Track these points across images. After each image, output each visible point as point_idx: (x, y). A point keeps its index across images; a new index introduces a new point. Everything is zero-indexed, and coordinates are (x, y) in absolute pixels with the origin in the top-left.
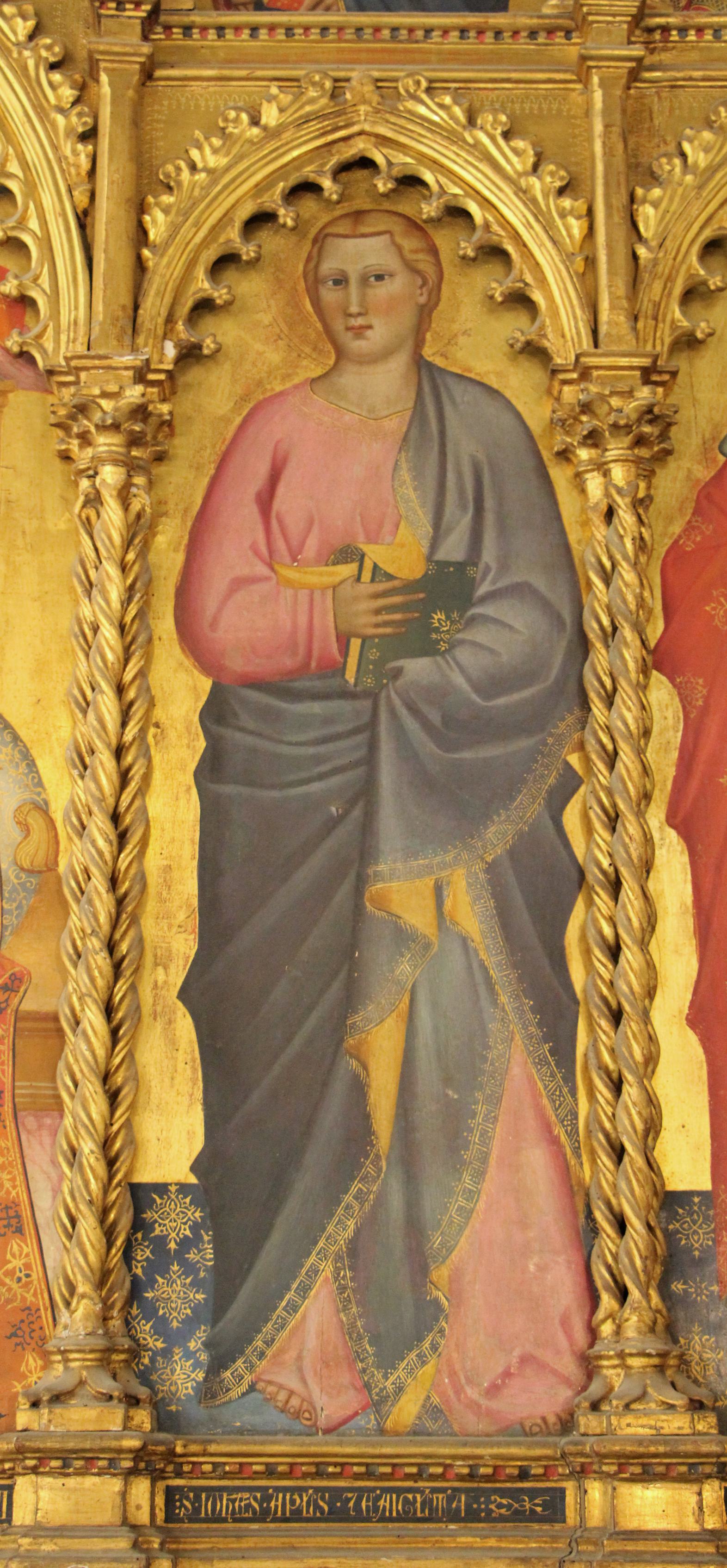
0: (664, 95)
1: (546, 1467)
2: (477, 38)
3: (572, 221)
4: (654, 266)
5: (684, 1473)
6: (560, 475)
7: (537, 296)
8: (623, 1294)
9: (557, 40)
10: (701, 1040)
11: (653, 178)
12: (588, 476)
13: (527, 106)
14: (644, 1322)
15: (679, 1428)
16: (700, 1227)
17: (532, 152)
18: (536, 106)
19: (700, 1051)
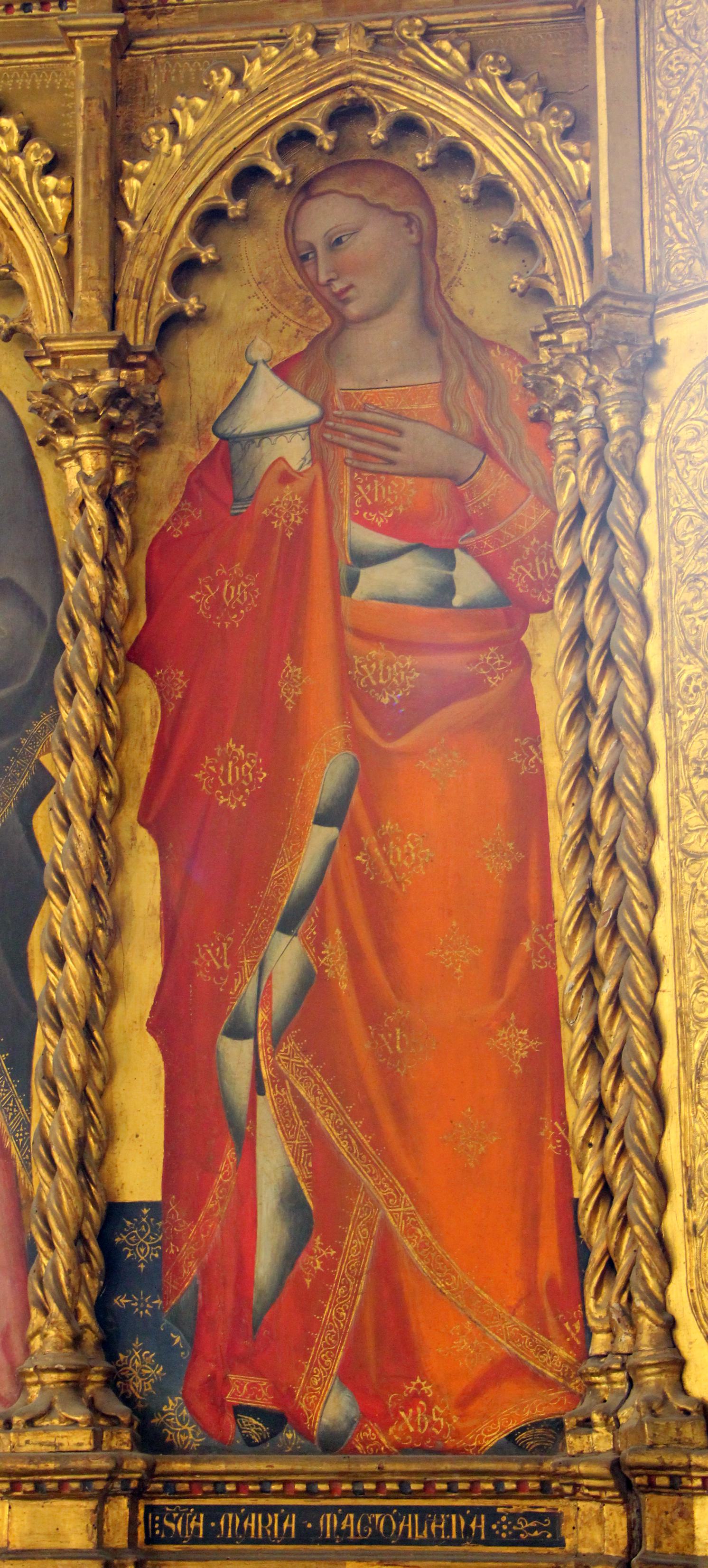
0: (160, 61)
3: (54, 199)
4: (136, 243)
5: (77, 1490)
7: (22, 279)
9: (52, 11)
10: (160, 1046)
11: (141, 151)
12: (66, 465)
13: (19, 82)
14: (61, 1337)
15: (80, 1444)
16: (148, 1239)
17: (16, 131)
18: (29, 82)
19: (160, 1057)
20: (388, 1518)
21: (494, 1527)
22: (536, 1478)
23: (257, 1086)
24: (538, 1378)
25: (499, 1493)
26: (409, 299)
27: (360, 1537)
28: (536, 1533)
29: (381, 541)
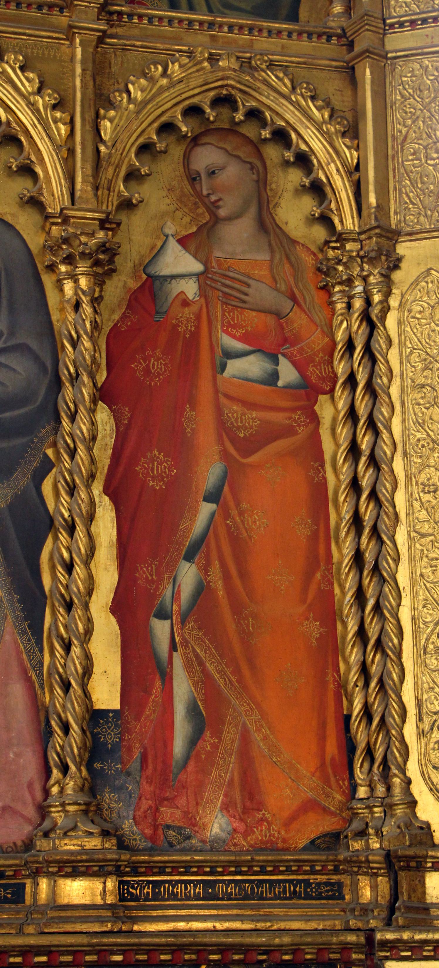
0: (118, 53)
1: (15, 871)
2: (5, 5)
4: (109, 158)
5: (96, 871)
6: (48, 280)
7: (38, 170)
8: (65, 769)
9: (55, 13)
10: (117, 621)
11: (110, 104)
12: (65, 282)
13: (35, 51)
14: (77, 785)
15: (95, 846)
16: (112, 731)
17: (37, 81)
18: (41, 52)
19: (117, 628)
20: (252, 886)
21: (309, 890)
22: (332, 863)
23: (173, 647)
24: (325, 810)
25: (313, 872)
26: (253, 211)
27: (238, 897)
28: (330, 893)
29: (238, 346)
